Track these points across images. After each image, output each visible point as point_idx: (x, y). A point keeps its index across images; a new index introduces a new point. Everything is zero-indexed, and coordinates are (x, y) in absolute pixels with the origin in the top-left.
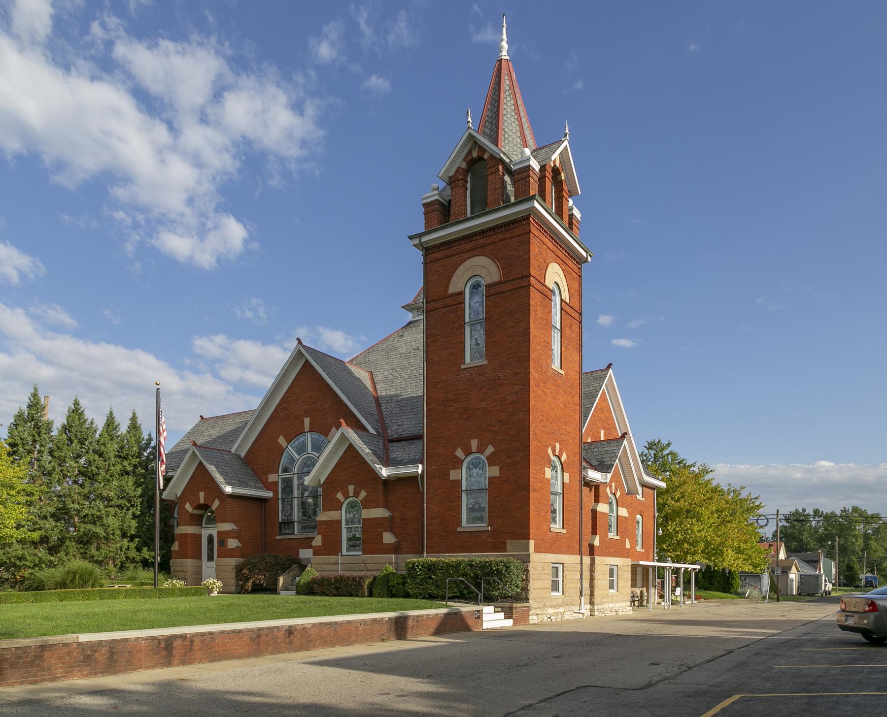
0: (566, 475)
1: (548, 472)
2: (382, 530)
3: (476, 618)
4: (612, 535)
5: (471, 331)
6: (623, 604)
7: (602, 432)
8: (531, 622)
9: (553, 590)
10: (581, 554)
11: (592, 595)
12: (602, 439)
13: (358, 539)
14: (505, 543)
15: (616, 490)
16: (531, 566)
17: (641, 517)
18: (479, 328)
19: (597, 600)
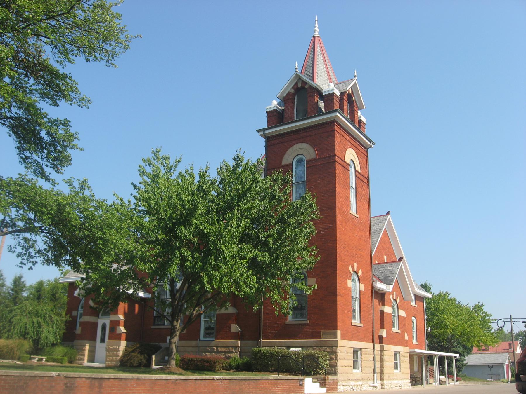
0: (362, 286)
1: (350, 283)
2: (231, 322)
3: (300, 385)
4: (395, 329)
5: (296, 188)
6: (405, 381)
7: (385, 257)
8: (339, 391)
9: (354, 368)
10: (373, 342)
11: (382, 372)
12: (386, 261)
13: (213, 329)
14: (320, 333)
15: (397, 297)
16: (339, 350)
17: (415, 319)
18: (302, 187)
19: (386, 376)
